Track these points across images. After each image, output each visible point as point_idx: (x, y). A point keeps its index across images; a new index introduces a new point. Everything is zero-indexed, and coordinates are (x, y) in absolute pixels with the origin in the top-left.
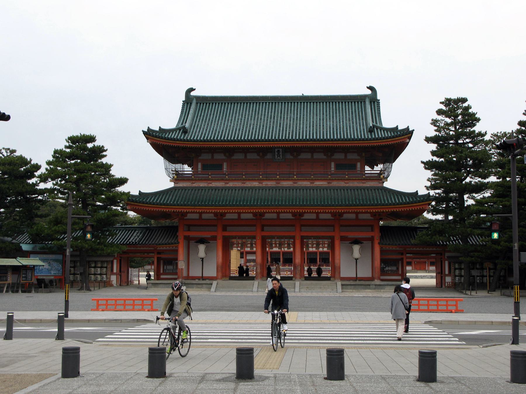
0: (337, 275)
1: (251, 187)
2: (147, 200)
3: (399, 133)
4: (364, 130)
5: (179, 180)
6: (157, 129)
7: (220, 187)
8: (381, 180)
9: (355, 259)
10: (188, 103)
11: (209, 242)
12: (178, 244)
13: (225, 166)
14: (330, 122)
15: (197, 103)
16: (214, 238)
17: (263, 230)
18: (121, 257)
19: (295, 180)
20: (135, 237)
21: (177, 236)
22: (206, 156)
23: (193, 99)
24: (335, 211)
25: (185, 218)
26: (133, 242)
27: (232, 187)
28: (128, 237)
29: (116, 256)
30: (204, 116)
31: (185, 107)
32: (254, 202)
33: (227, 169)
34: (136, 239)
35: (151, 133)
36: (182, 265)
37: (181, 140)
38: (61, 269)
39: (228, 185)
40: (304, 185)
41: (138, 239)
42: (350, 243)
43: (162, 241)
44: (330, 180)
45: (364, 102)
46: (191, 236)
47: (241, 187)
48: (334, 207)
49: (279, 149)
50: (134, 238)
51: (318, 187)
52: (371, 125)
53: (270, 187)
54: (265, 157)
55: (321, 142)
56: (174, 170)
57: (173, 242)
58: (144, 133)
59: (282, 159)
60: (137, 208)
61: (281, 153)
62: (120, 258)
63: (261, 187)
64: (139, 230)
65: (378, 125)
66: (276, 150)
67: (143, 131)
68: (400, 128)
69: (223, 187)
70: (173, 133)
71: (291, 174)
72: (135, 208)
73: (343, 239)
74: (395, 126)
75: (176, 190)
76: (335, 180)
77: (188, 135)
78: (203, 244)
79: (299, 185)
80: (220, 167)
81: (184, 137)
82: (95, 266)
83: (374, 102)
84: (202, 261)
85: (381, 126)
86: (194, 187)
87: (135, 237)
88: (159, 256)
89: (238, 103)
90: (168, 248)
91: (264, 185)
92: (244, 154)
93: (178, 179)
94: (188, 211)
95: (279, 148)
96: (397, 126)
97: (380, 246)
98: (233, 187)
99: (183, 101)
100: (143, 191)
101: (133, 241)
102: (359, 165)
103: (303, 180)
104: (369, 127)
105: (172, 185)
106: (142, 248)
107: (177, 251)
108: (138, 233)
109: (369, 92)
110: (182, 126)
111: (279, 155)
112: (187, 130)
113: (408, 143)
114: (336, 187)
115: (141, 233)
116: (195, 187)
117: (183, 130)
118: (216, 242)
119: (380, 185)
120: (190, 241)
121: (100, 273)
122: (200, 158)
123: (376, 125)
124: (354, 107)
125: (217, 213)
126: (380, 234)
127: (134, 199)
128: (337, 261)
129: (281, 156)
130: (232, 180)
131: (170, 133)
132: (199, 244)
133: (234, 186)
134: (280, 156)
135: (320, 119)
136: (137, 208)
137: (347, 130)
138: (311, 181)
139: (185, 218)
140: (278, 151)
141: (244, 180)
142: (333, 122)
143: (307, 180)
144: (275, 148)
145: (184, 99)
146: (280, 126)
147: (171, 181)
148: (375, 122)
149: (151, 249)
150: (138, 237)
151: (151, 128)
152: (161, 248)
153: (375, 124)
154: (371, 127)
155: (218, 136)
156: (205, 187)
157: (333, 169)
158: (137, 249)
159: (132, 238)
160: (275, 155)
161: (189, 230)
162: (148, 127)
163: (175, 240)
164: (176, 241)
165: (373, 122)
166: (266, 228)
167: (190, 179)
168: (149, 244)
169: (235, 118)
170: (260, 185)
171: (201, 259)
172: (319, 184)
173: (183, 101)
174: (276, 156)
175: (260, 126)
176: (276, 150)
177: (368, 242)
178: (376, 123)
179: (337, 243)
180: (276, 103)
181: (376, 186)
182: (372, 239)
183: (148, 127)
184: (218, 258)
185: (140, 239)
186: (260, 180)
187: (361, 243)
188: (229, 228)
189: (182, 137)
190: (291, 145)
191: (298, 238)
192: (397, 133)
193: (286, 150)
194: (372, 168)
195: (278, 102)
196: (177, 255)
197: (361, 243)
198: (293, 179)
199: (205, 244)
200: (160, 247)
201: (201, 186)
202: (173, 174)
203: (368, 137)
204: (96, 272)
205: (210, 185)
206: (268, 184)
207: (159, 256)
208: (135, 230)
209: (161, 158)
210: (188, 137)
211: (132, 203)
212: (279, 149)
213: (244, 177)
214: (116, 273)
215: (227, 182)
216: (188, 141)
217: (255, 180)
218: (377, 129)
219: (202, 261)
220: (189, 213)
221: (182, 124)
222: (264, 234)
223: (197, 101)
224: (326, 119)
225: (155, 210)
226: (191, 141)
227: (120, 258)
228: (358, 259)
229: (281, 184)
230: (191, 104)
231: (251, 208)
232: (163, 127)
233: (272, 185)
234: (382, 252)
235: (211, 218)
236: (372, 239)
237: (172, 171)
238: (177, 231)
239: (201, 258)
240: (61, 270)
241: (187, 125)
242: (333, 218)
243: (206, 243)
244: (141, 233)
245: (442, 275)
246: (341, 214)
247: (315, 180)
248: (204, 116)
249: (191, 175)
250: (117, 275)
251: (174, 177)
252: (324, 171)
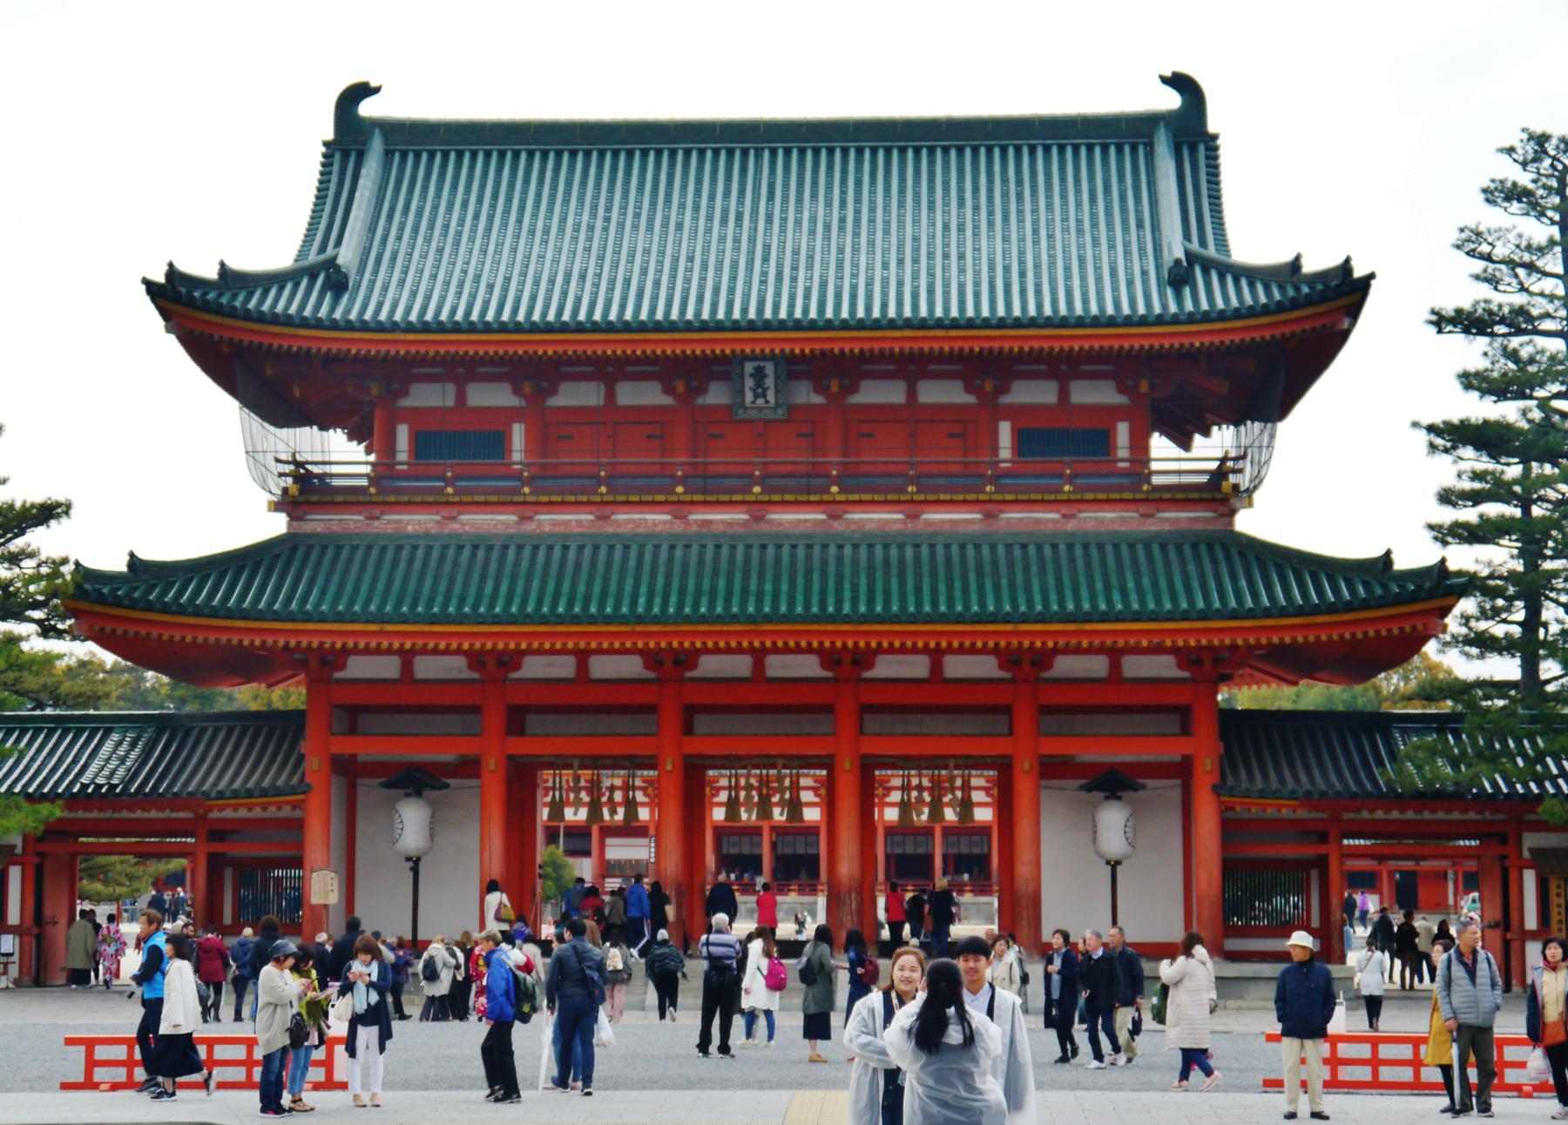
0: (1024, 931)
1: (638, 535)
2: (165, 592)
3: (1305, 290)
4: (1144, 273)
5: (307, 503)
6: (211, 273)
7: (497, 536)
8: (1225, 500)
9: (1108, 862)
10: (345, 156)
11: (446, 786)
12: (304, 793)
13: (518, 433)
14: (991, 238)
15: (388, 154)
16: (469, 768)
17: (688, 729)
18: (40, 854)
19: (835, 502)
20: (108, 760)
21: (301, 758)
22: (430, 396)
23: (371, 131)
24: (1015, 643)
25: (338, 675)
26: (100, 786)
27: (550, 535)
28: (75, 761)
29: (19, 850)
30: (420, 213)
31: (336, 168)
32: (649, 604)
33: (527, 452)
34: (113, 773)
35: (183, 290)
36: (323, 888)
37: (318, 324)
39: (530, 527)
40: (873, 526)
41: (121, 772)
42: (1082, 788)
43: (232, 781)
44: (991, 501)
45: (1145, 145)
46: (361, 758)
47: (591, 536)
48: (1009, 627)
49: (762, 364)
50: (102, 768)
51: (936, 533)
52: (1179, 254)
53: (724, 534)
54: (700, 401)
55: (952, 333)
56: (283, 457)
57: (280, 782)
58: (152, 288)
59: (775, 409)
60: (120, 632)
61: (770, 382)
62: (36, 860)
63: (678, 536)
64: (126, 730)
65: (1211, 251)
66: (749, 367)
67: (146, 282)
68: (1309, 267)
69: (511, 537)
70: (281, 289)
71: (815, 476)
72: (108, 629)
73: (1053, 769)
74: (1285, 257)
75: (294, 549)
76: (1016, 502)
77: (352, 301)
78: (418, 794)
79: (853, 527)
80: (501, 444)
81: (333, 309)
83: (1193, 149)
84: (415, 870)
85: (1222, 258)
87: (108, 760)
88: (218, 848)
89: (573, 154)
90: (258, 813)
91: (695, 528)
92: (602, 387)
93: (302, 499)
94: (350, 644)
95: (763, 357)
96: (1298, 258)
97: (1222, 803)
98: (557, 535)
99: (326, 144)
100: (146, 554)
101: (100, 781)
102: (1123, 431)
103: (872, 502)
104: (1168, 260)
105: (277, 525)
106: (139, 814)
107: (299, 824)
108: (119, 744)
109: (1171, 100)
110: (322, 257)
111: (759, 391)
112: (346, 277)
113: (1343, 336)
114: (1017, 535)
115: (133, 745)
116: (383, 536)
117: (328, 278)
118: (474, 782)
119: (1218, 526)
120: (360, 781)
122: (406, 403)
123: (1202, 251)
124: (1102, 169)
125: (482, 651)
126: (1222, 744)
127: (105, 591)
128: (1023, 869)
129: (771, 397)
130: (550, 503)
131: (266, 292)
132: (396, 800)
133: (557, 530)
134: (764, 395)
135: (946, 227)
136: (120, 632)
137: (1068, 278)
138: (907, 508)
139: (338, 675)
140: (759, 374)
141: (603, 503)
142: (1006, 239)
143: (886, 502)
144: (745, 358)
145: (330, 135)
146: (766, 259)
147: (277, 507)
148: (1195, 238)
149: (182, 815)
150: (123, 760)
151: (184, 267)
152: (228, 814)
153: (1195, 246)
154: (1178, 262)
155: (486, 304)
156: (427, 536)
157: (1005, 453)
158: (116, 815)
159: (93, 768)
160: (742, 392)
161: (353, 730)
162: (171, 265)
163: (291, 775)
164: (295, 780)
165: (1187, 236)
166: (703, 723)
167: (361, 498)
168: (174, 794)
169: (563, 220)
170: (678, 527)
171: (411, 864)
172: (943, 522)
173: (326, 144)
174: (749, 397)
175: (675, 260)
176: (749, 367)
177: (1167, 782)
178: (1203, 243)
179: (1023, 785)
180: (745, 152)
181: (1200, 527)
182: (1182, 771)
183: (171, 265)
184: (487, 855)
185: (129, 770)
186: (679, 507)
187: (1136, 788)
188: (534, 722)
189: (323, 313)
190: (817, 347)
191: (847, 766)
192: (1297, 289)
193: (794, 367)
194: (1185, 444)
195: (756, 150)
196: (300, 845)
197: (1136, 789)
198: (825, 498)
199: (427, 793)
200: (222, 808)
201: (410, 528)
202: (281, 475)
203: (1164, 306)
205: (456, 526)
206: (710, 522)
207: (218, 848)
208: (108, 733)
209: (226, 406)
210: (350, 308)
211: (98, 609)
212: (762, 364)
213: (603, 489)
214: (21, 926)
215: (528, 511)
216: (349, 326)
217: (654, 503)
218: (1206, 272)
219: (415, 870)
220: (356, 651)
221: (323, 249)
222: (693, 746)
223: (386, 141)
224: (976, 227)
225: (200, 639)
226: (364, 326)
227: (36, 860)
228: (1118, 863)
229: (770, 522)
230: (361, 156)
231: (639, 628)
232: (238, 264)
234: (1230, 827)
235: (453, 676)
236: (1182, 771)
237: (278, 461)
238: (299, 735)
239: (408, 859)
241: (347, 256)
242: (1006, 675)
243: (434, 788)
244: (133, 745)
245: (1509, 936)
246: (1044, 658)
247: (926, 502)
248: (420, 213)
249: (364, 482)
250: (21, 936)
251: (285, 490)
252: (965, 464)
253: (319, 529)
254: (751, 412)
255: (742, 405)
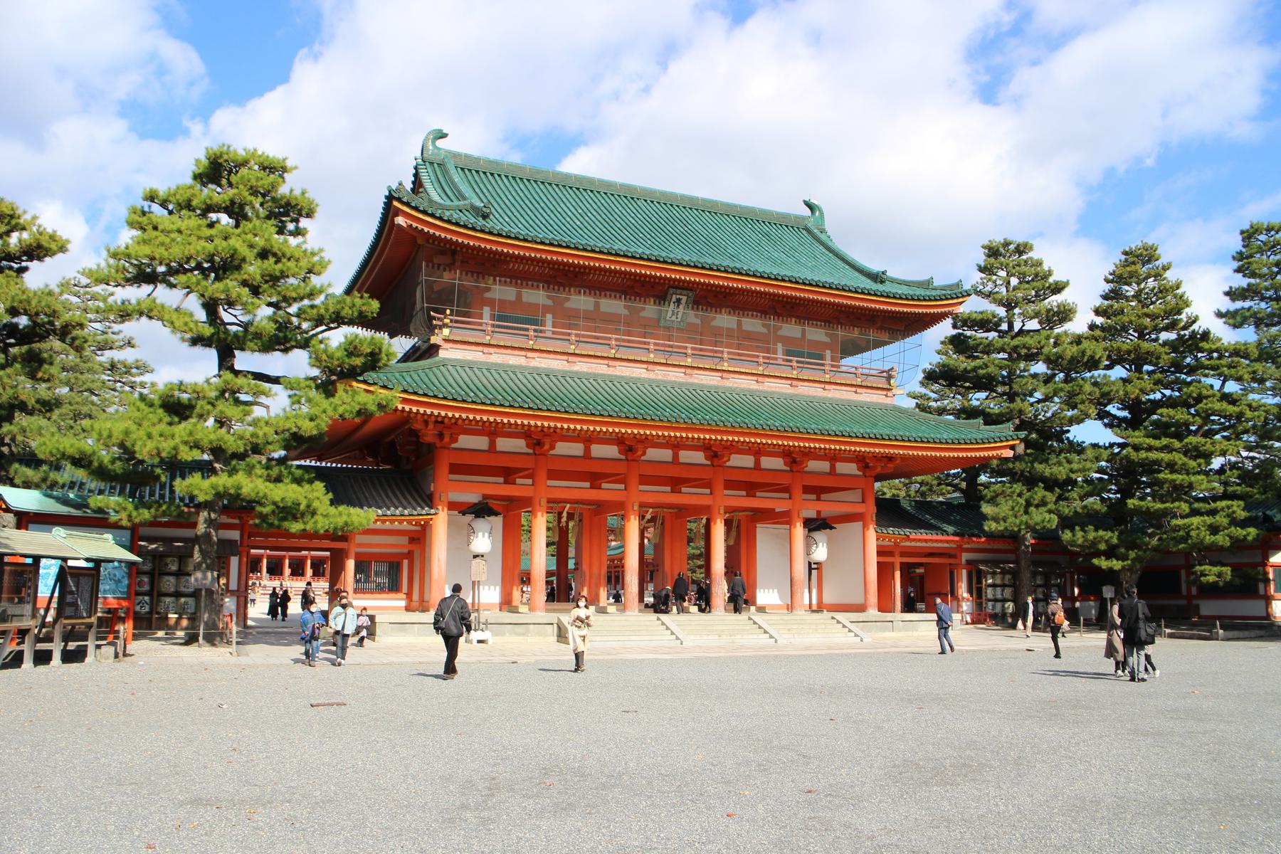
1: (632, 378)
7: (559, 370)
27: (587, 373)
38: (123, 577)
53: (675, 382)
59: (680, 322)
79: (736, 385)
82: (179, 569)
86: (492, 363)
91: (660, 378)
114: (809, 396)
121: (177, 592)
187: (831, 528)
201: (511, 362)
204: (182, 589)
212: (681, 297)
214: (238, 590)
233: (702, 380)
240: (126, 582)
253: (459, 357)
254: (669, 323)
255: (665, 319)
